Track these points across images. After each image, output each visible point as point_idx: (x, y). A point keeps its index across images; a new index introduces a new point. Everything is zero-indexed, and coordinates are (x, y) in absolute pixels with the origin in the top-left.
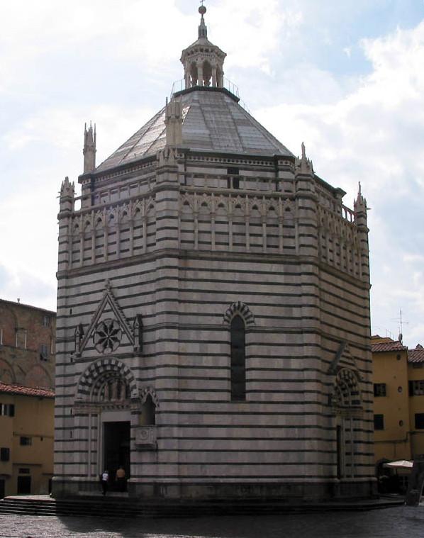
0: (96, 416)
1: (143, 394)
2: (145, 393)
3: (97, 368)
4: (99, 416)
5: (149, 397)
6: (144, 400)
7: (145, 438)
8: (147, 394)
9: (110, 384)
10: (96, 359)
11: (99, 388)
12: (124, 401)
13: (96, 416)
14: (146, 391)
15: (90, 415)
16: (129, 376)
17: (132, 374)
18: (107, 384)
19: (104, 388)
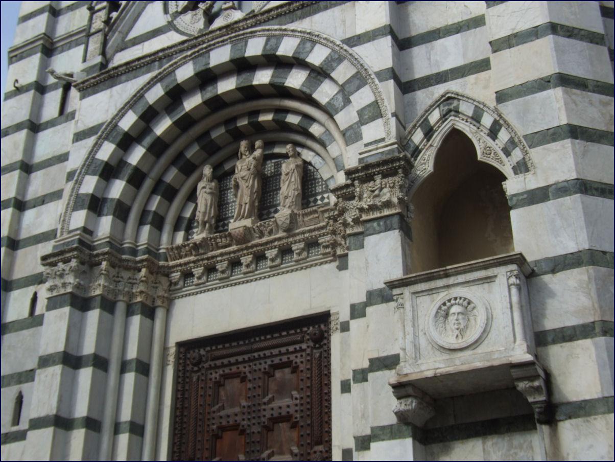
0: (149, 313)
1: (418, 137)
2: (429, 133)
3: (176, 94)
4: (160, 314)
5: (457, 146)
6: (425, 165)
7: (472, 335)
8: (437, 140)
9: (222, 176)
10: (169, 57)
11: (170, 194)
12: (293, 217)
13: (149, 313)
14: (435, 117)
15: (121, 308)
16: (343, 72)
17: (355, 61)
18: (207, 170)
19: (192, 196)
